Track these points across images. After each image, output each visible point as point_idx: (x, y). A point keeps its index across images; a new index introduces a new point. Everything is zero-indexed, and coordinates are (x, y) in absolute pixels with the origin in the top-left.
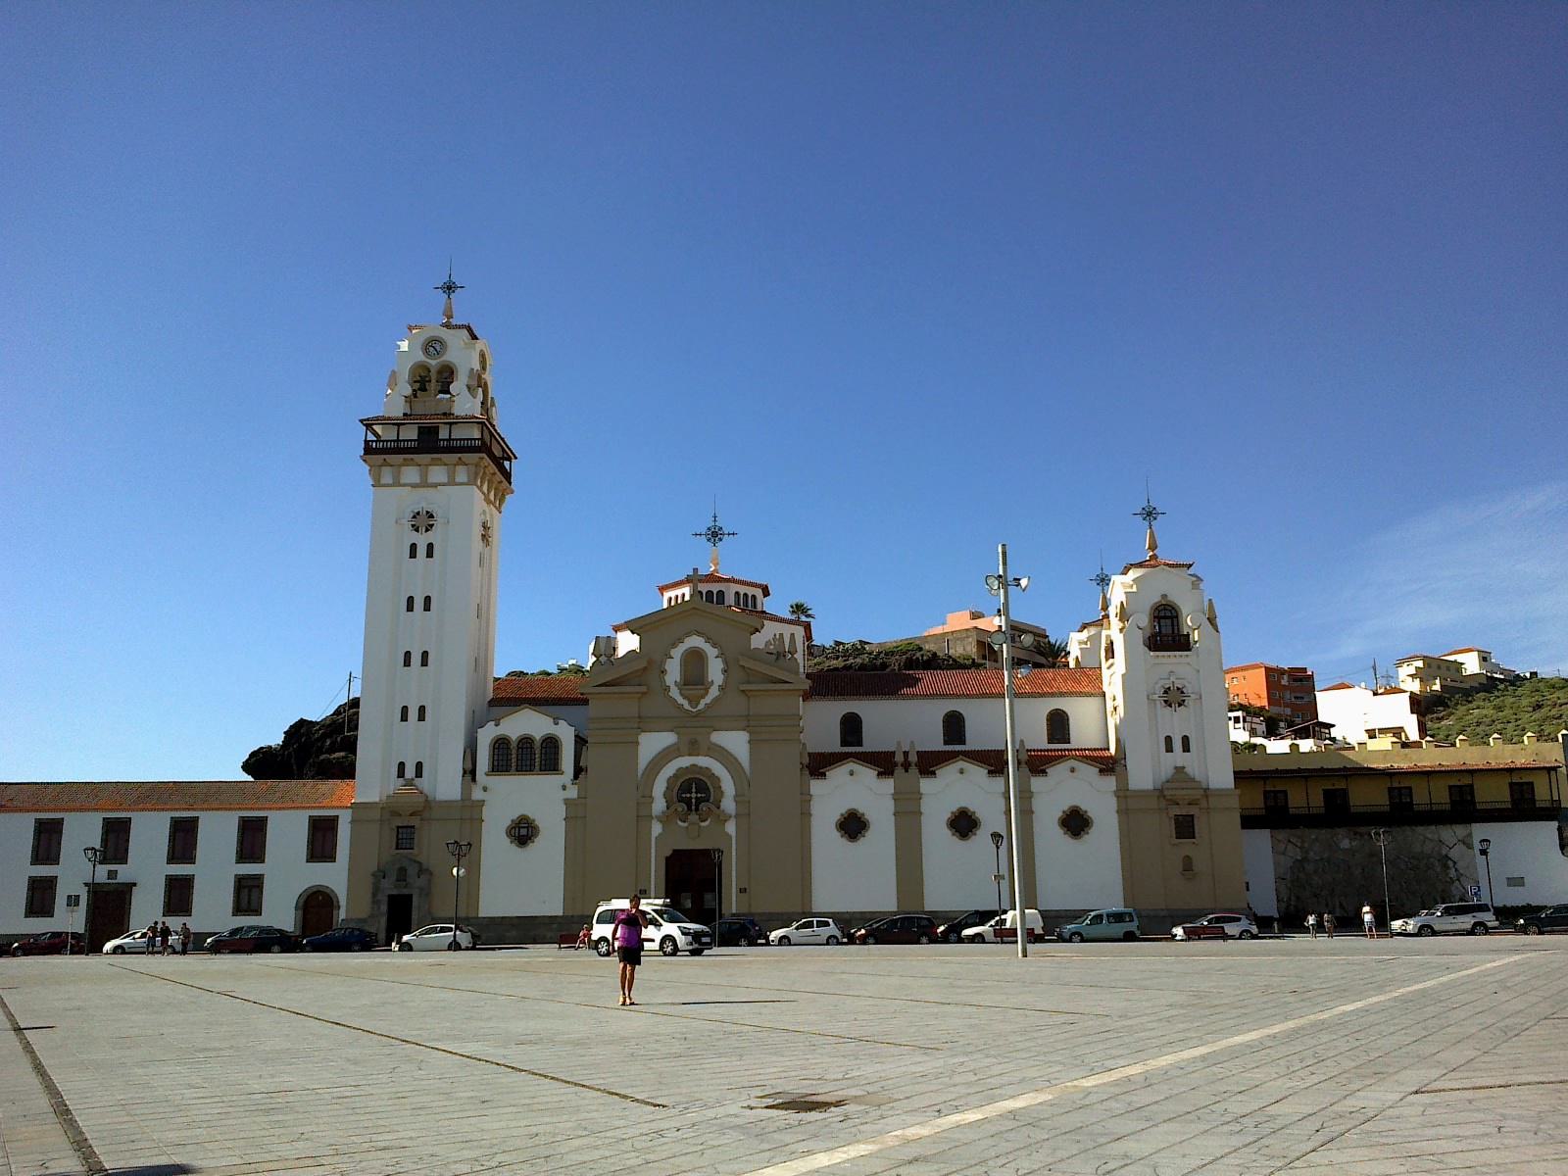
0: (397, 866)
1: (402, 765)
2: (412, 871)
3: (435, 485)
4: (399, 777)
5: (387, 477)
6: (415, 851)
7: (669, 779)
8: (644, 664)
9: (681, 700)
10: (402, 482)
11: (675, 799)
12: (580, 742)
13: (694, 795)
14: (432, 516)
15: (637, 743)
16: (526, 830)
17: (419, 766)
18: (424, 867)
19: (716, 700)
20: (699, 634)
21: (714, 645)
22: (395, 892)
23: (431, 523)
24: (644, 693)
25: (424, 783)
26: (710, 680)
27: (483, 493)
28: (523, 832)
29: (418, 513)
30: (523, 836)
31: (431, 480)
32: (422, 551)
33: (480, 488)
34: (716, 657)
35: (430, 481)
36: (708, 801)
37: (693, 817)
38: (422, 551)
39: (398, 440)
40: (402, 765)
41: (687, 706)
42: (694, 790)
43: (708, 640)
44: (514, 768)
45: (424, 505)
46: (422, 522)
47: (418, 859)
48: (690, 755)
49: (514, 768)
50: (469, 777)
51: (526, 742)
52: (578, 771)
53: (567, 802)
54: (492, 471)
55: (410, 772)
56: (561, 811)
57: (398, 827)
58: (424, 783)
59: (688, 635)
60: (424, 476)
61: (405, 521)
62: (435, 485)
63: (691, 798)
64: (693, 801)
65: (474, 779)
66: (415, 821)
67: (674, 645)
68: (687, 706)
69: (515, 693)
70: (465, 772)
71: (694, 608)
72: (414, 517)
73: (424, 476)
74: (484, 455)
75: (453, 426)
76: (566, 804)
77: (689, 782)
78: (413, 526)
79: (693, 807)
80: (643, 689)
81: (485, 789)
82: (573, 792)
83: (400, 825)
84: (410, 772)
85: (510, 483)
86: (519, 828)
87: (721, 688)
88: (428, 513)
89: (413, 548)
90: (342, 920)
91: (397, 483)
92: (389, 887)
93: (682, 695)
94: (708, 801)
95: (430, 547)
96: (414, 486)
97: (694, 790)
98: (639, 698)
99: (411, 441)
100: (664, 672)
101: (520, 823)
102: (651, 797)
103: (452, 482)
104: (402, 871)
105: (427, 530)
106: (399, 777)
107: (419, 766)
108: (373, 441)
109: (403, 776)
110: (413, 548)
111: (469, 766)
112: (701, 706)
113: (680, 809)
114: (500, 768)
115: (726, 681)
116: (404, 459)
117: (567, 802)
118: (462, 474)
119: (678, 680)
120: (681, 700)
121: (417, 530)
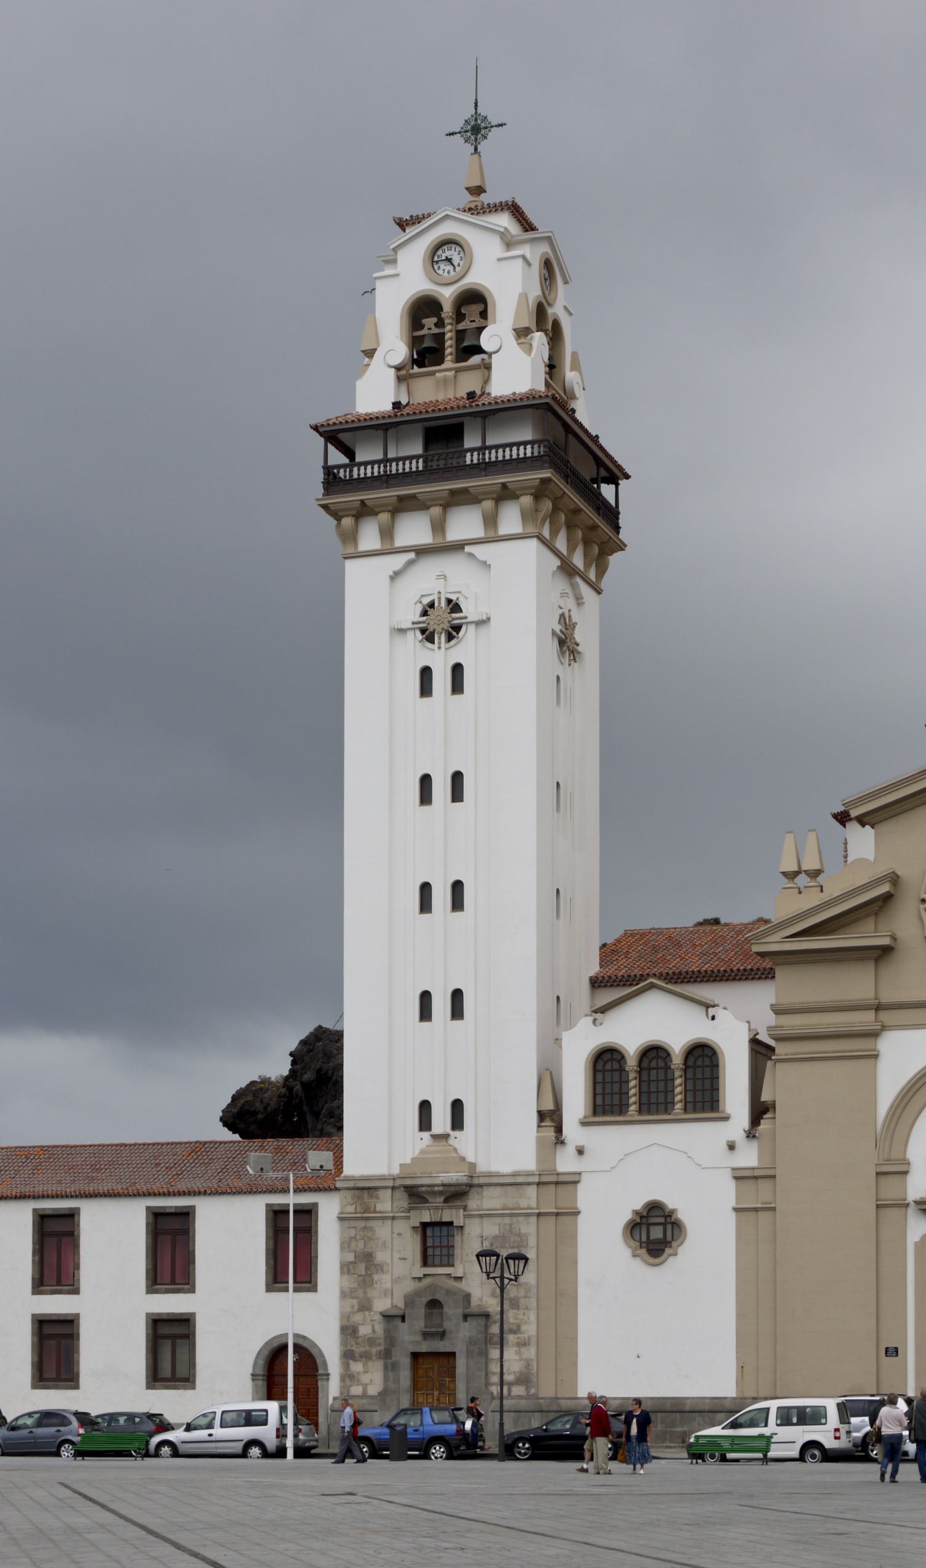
0: (425, 1300)
1: (425, 1107)
2: (452, 1311)
3: (458, 547)
4: (421, 1129)
6: (458, 1271)
10: (400, 541)
12: (760, 1051)
14: (454, 607)
16: (661, 1228)
17: (457, 1107)
18: (474, 1302)
22: (424, 1348)
27: (556, 553)
28: (657, 1233)
29: (432, 605)
30: (657, 1242)
32: (441, 680)
33: (549, 545)
38: (441, 680)
40: (425, 1107)
45: (440, 585)
46: (440, 619)
47: (463, 1285)
50: (550, 1133)
51: (654, 1053)
52: (760, 1111)
53: (741, 1177)
54: (572, 507)
56: (727, 1193)
57: (425, 1226)
58: (465, 1143)
60: (439, 527)
62: (458, 547)
65: (559, 1129)
70: (542, 1116)
72: (425, 613)
73: (439, 527)
76: (737, 1178)
82: (749, 1157)
83: (428, 1220)
85: (617, 528)
86: (649, 1225)
88: (449, 601)
89: (426, 674)
90: (335, 1399)
92: (410, 1338)
96: (421, 552)
101: (647, 1217)
104: (434, 1305)
105: (450, 638)
106: (421, 1129)
107: (457, 1107)
108: (339, 467)
110: (426, 674)
117: (741, 1177)
118: (511, 519)
121: (430, 639)
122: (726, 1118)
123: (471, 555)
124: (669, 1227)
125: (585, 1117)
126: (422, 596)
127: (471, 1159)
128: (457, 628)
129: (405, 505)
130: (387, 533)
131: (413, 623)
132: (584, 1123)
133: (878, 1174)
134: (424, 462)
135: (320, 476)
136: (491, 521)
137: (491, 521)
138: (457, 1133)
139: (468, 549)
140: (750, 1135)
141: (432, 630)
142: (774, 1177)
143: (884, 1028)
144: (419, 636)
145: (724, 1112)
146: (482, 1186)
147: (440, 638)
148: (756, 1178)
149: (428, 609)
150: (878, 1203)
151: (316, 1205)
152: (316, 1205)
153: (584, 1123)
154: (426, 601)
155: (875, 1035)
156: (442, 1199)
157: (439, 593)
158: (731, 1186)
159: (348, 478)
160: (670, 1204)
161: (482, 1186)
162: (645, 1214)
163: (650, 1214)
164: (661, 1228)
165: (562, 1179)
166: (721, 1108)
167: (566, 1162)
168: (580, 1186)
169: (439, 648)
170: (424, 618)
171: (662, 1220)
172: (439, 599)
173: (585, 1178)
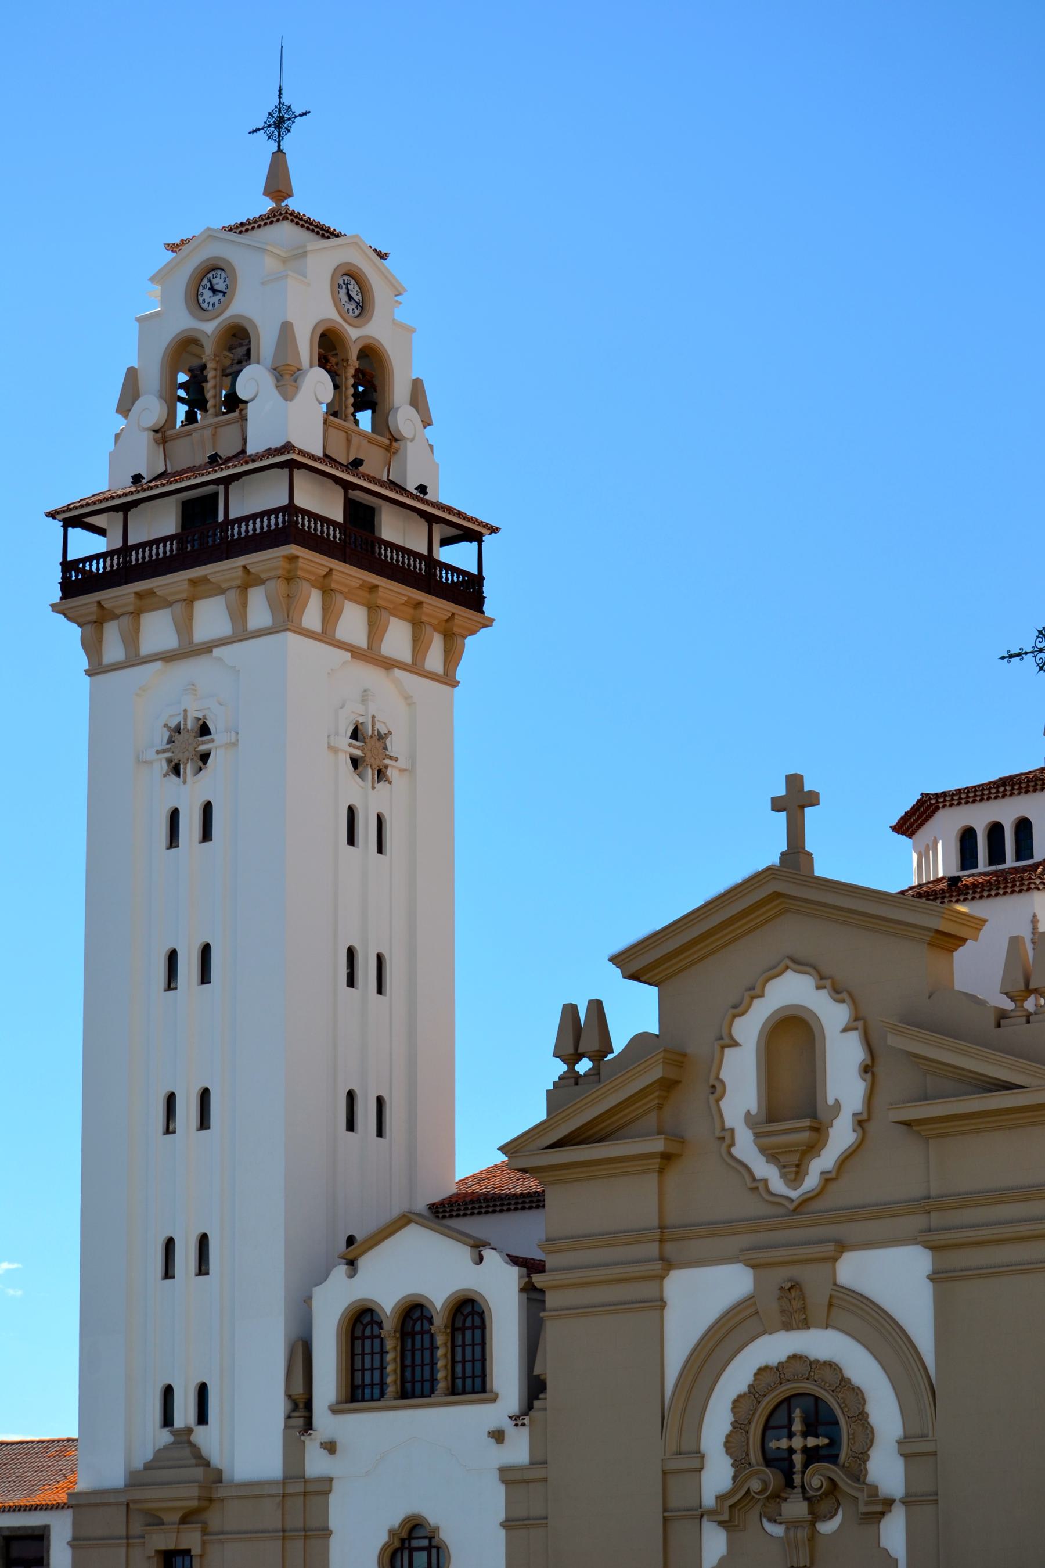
3: (207, 649)
5: (114, 650)
7: (736, 1402)
8: (657, 1073)
9: (764, 1170)
11: (755, 1455)
13: (797, 1443)
15: (660, 1304)
16: (424, 1554)
19: (846, 1159)
20: (799, 964)
21: (838, 991)
23: (203, 748)
24: (667, 1157)
25: (202, 1436)
26: (831, 1101)
31: (201, 633)
34: (845, 1030)
35: (201, 633)
36: (833, 1459)
37: (796, 1508)
38: (190, 825)
39: (125, 550)
41: (778, 1185)
42: (797, 1427)
43: (824, 980)
44: (441, 1386)
48: (788, 1327)
49: (441, 1386)
53: (510, 1477)
55: (184, 1412)
59: (774, 972)
60: (184, 626)
61: (151, 755)
62: (207, 649)
63: (791, 1451)
64: (798, 1459)
66: (191, 1539)
67: (739, 1009)
68: (778, 1185)
69: (456, 1183)
71: (778, 895)
72: (170, 741)
73: (184, 626)
74: (293, 549)
75: (233, 487)
76: (506, 1482)
77: (788, 1401)
78: (169, 761)
79: (797, 1478)
80: (657, 1145)
81: (330, 1447)
84: (184, 1412)
86: (412, 1550)
87: (861, 1123)
91: (134, 659)
93: (763, 1150)
94: (833, 1459)
95: (207, 809)
96: (168, 657)
97: (797, 1427)
98: (661, 1171)
99: (164, 540)
100: (716, 1089)
102: (698, 1452)
103: (242, 634)
109: (172, 1425)
111: (299, 1389)
112: (811, 1181)
113: (755, 1485)
114: (418, 1391)
115: (870, 1098)
116: (139, 595)
117: (510, 1477)
119: (754, 1111)
120: (764, 1170)
121: (176, 770)
122: (494, 1400)
123: (220, 659)
124: (434, 1551)
125: (337, 1403)
126: (170, 716)
127: (216, 1459)
128: (205, 757)
129: (146, 602)
130: (131, 640)
131: (158, 752)
132: (335, 1410)
133: (665, 1473)
134: (178, 543)
135: (57, 575)
136: (239, 613)
137: (239, 613)
138: (202, 1428)
139: (217, 652)
140: (517, 1420)
141: (176, 761)
142: (545, 1480)
143: (668, 1264)
144: (165, 767)
145: (492, 1391)
146: (223, 1500)
147: (185, 769)
148: (527, 1482)
149: (173, 734)
150: (666, 1514)
151: (46, 1528)
152: (46, 1528)
153: (335, 1410)
154: (173, 724)
155: (662, 1278)
156: (176, 1517)
157: (185, 711)
158: (499, 1491)
159: (101, 571)
160: (433, 1519)
161: (223, 1500)
162: (404, 1535)
163: (414, 1535)
164: (424, 1554)
165: (311, 1488)
166: (488, 1387)
167: (316, 1464)
168: (333, 1498)
169: (185, 782)
170: (169, 746)
171: (425, 1543)
172: (185, 720)
173: (335, 1484)
